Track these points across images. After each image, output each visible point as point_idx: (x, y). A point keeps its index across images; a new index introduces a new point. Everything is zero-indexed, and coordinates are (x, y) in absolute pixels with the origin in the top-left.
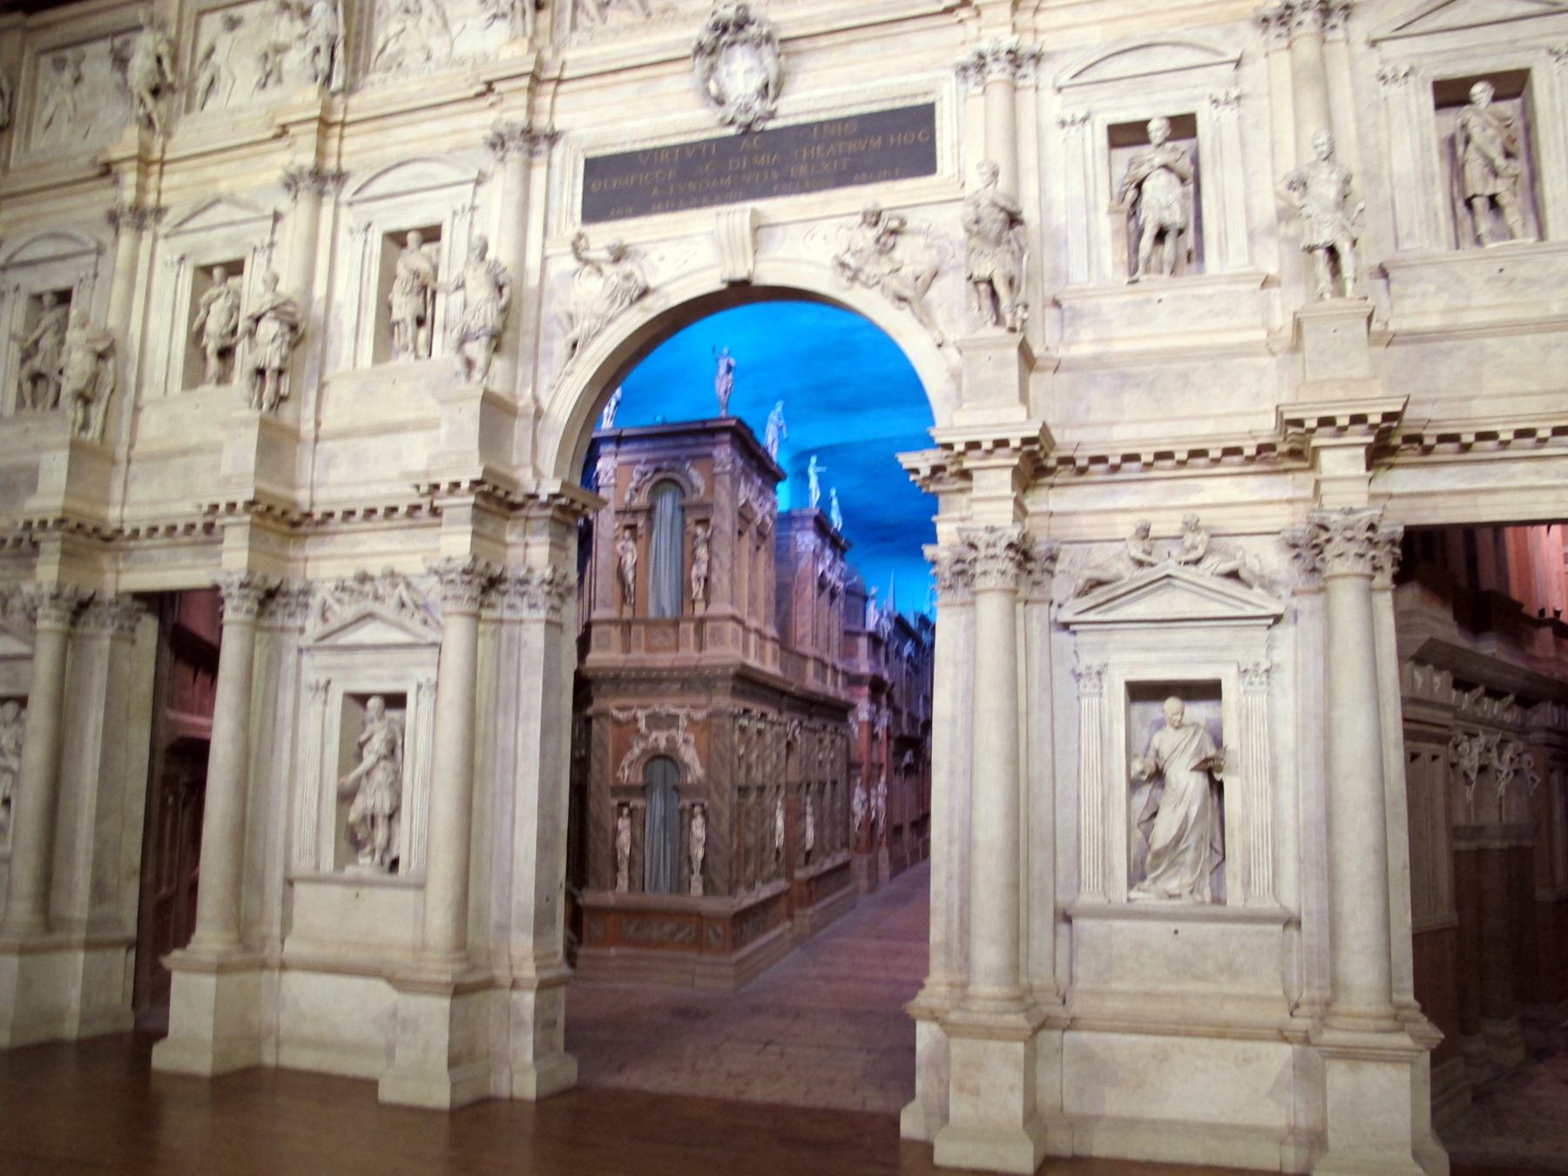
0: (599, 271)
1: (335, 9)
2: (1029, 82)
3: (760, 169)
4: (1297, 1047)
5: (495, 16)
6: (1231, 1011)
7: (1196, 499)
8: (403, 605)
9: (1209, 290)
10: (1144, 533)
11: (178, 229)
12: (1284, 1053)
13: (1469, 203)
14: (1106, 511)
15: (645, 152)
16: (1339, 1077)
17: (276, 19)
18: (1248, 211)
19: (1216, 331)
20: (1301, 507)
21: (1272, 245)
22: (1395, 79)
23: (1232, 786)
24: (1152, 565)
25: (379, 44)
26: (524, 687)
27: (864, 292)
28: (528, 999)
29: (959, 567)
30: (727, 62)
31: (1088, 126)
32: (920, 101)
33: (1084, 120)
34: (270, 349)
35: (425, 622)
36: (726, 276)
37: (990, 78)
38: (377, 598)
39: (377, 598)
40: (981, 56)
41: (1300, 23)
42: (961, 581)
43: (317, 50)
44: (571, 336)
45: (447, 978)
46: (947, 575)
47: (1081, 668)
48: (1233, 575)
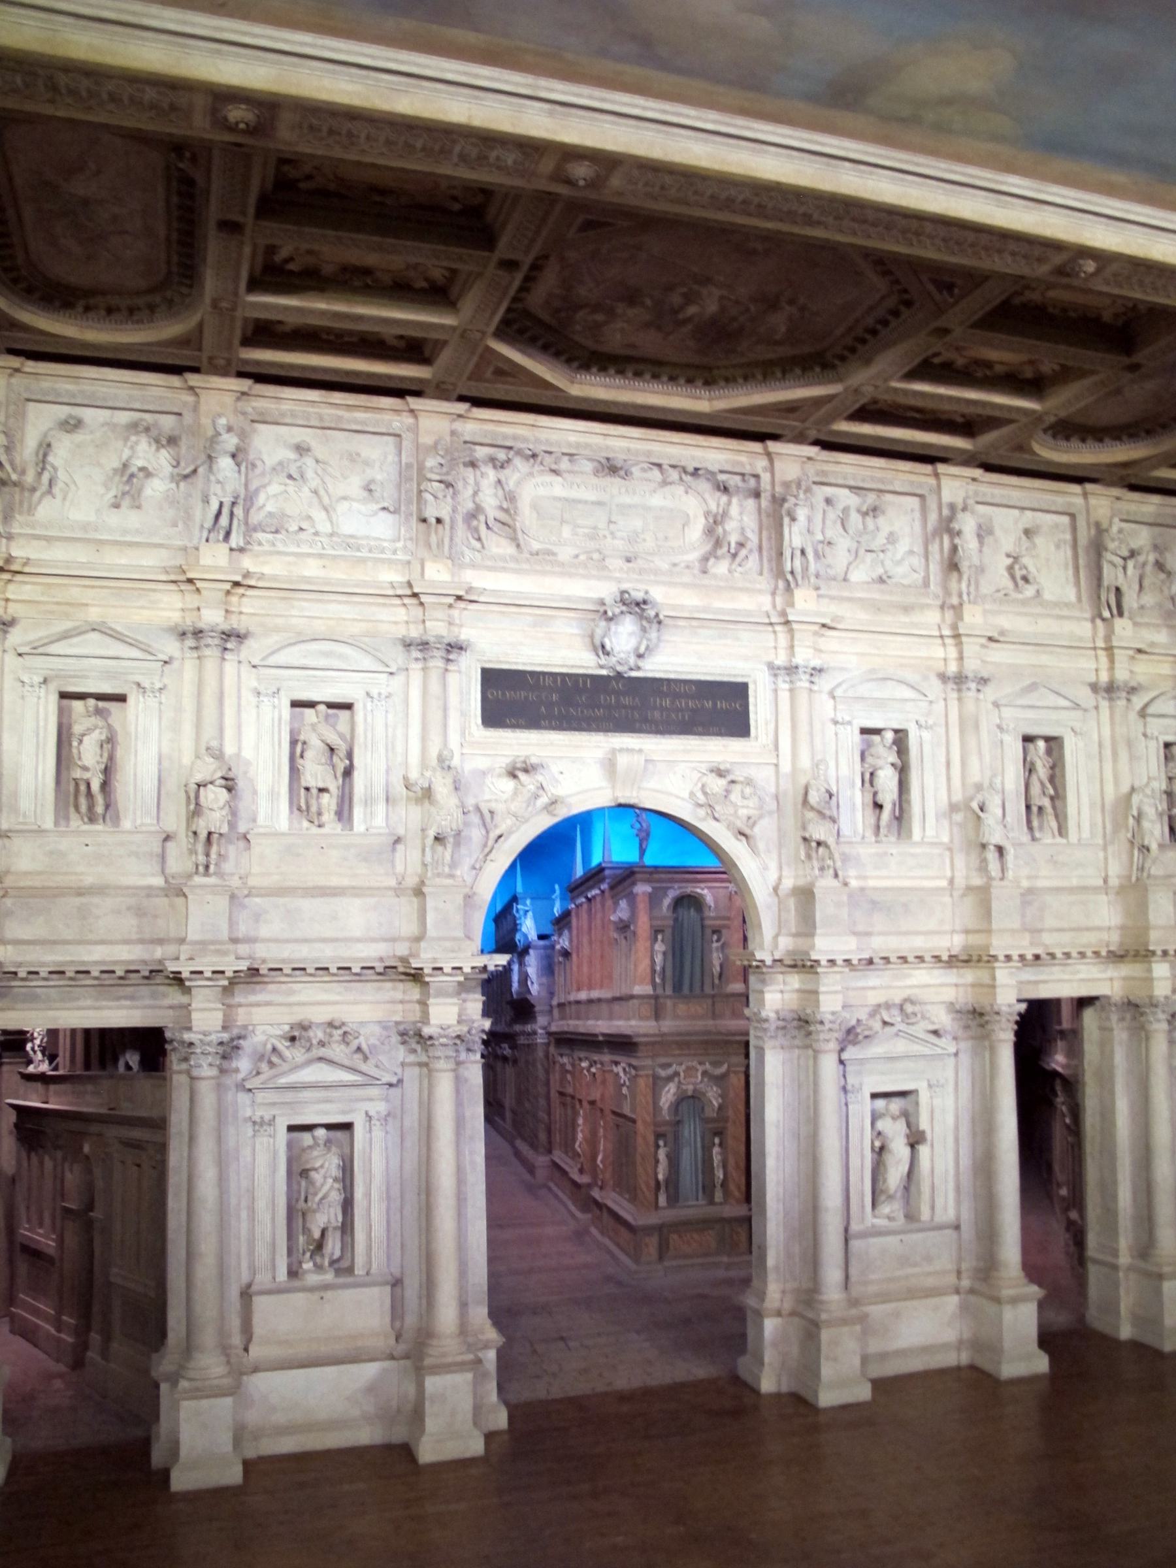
0: (515, 776)
1: (239, 472)
2: (815, 688)
3: (625, 707)
4: (963, 1296)
5: (384, 509)
6: (930, 1282)
7: (909, 982)
8: (359, 1049)
9: (918, 850)
10: (888, 1006)
11: (37, 650)
12: (954, 1300)
13: (1028, 807)
14: (864, 988)
15: (532, 673)
16: (1009, 1314)
17: (133, 438)
18: (936, 800)
19: (921, 878)
20: (961, 989)
21: (946, 823)
22: (1007, 731)
23: (924, 1151)
24: (892, 1025)
25: (261, 499)
26: (468, 1114)
27: (715, 823)
28: (491, 1355)
29: (781, 1023)
30: (616, 624)
31: (849, 727)
32: (739, 680)
33: (849, 723)
34: (217, 815)
35: (377, 1066)
36: (622, 801)
37: (799, 684)
38: (322, 1044)
39: (322, 1044)
40: (797, 667)
41: (969, 689)
42: (780, 1033)
43: (221, 504)
44: (498, 832)
45: (471, 1357)
46: (773, 1027)
47: (849, 1087)
48: (935, 1033)
